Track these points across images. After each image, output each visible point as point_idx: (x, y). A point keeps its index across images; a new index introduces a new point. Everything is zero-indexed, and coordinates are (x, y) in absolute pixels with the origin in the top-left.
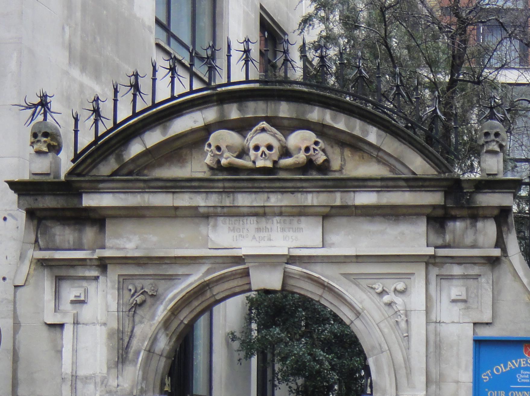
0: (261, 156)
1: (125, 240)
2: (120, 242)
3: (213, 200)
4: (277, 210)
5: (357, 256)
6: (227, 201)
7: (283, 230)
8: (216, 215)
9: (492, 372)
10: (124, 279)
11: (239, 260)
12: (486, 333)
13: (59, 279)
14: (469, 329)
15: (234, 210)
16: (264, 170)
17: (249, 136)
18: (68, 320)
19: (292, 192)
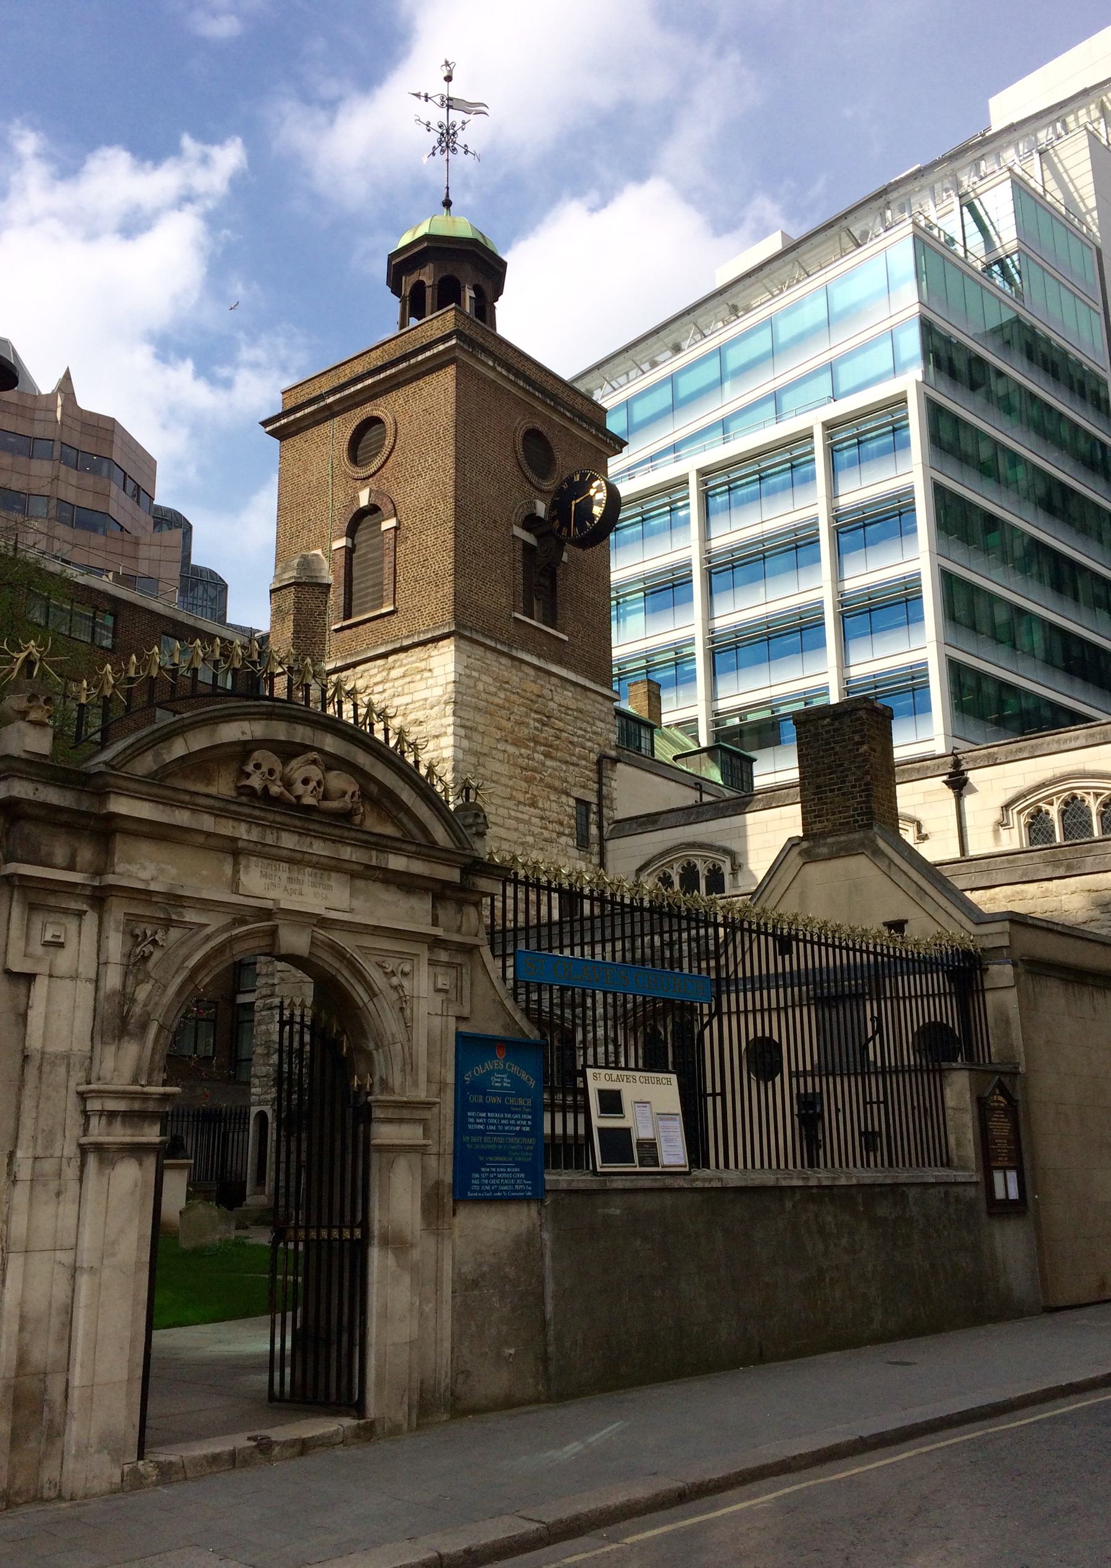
0: (312, 792)
1: (138, 866)
2: (133, 868)
3: (255, 835)
4: (315, 859)
5: (376, 927)
6: (270, 839)
7: (314, 885)
8: (252, 853)
9: (473, 1074)
10: (132, 919)
11: (266, 914)
12: (464, 1028)
13: (33, 907)
14: (452, 1024)
15: (274, 851)
16: (310, 808)
17: (294, 763)
18: (42, 969)
19: (334, 841)
